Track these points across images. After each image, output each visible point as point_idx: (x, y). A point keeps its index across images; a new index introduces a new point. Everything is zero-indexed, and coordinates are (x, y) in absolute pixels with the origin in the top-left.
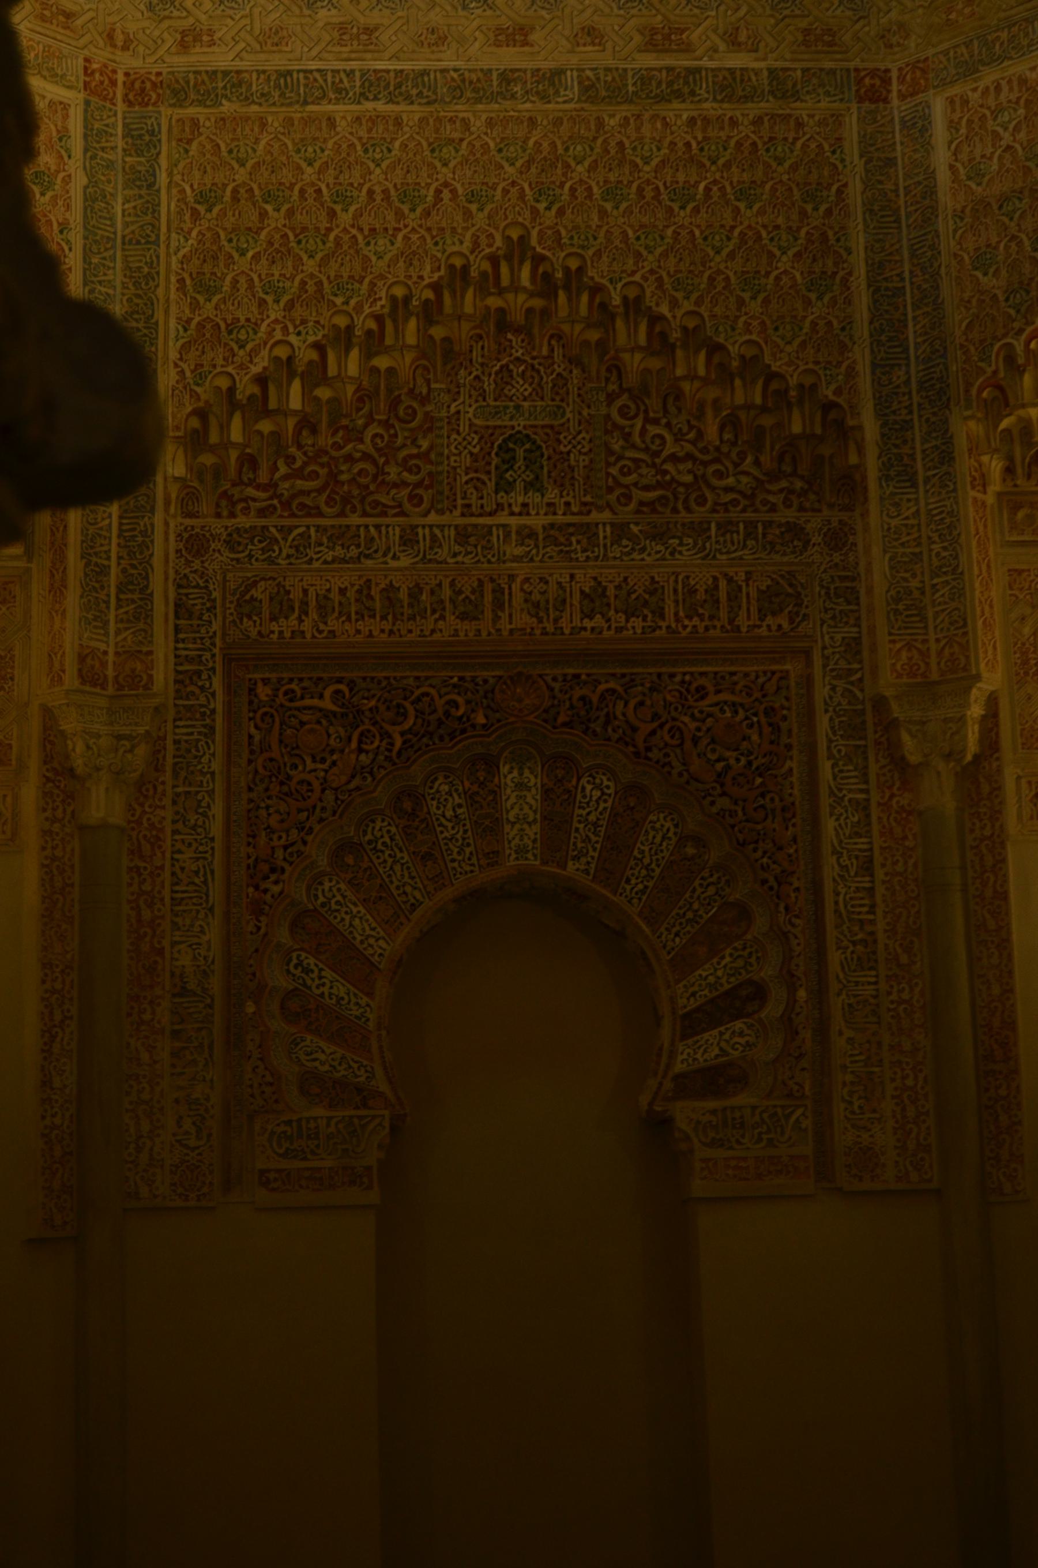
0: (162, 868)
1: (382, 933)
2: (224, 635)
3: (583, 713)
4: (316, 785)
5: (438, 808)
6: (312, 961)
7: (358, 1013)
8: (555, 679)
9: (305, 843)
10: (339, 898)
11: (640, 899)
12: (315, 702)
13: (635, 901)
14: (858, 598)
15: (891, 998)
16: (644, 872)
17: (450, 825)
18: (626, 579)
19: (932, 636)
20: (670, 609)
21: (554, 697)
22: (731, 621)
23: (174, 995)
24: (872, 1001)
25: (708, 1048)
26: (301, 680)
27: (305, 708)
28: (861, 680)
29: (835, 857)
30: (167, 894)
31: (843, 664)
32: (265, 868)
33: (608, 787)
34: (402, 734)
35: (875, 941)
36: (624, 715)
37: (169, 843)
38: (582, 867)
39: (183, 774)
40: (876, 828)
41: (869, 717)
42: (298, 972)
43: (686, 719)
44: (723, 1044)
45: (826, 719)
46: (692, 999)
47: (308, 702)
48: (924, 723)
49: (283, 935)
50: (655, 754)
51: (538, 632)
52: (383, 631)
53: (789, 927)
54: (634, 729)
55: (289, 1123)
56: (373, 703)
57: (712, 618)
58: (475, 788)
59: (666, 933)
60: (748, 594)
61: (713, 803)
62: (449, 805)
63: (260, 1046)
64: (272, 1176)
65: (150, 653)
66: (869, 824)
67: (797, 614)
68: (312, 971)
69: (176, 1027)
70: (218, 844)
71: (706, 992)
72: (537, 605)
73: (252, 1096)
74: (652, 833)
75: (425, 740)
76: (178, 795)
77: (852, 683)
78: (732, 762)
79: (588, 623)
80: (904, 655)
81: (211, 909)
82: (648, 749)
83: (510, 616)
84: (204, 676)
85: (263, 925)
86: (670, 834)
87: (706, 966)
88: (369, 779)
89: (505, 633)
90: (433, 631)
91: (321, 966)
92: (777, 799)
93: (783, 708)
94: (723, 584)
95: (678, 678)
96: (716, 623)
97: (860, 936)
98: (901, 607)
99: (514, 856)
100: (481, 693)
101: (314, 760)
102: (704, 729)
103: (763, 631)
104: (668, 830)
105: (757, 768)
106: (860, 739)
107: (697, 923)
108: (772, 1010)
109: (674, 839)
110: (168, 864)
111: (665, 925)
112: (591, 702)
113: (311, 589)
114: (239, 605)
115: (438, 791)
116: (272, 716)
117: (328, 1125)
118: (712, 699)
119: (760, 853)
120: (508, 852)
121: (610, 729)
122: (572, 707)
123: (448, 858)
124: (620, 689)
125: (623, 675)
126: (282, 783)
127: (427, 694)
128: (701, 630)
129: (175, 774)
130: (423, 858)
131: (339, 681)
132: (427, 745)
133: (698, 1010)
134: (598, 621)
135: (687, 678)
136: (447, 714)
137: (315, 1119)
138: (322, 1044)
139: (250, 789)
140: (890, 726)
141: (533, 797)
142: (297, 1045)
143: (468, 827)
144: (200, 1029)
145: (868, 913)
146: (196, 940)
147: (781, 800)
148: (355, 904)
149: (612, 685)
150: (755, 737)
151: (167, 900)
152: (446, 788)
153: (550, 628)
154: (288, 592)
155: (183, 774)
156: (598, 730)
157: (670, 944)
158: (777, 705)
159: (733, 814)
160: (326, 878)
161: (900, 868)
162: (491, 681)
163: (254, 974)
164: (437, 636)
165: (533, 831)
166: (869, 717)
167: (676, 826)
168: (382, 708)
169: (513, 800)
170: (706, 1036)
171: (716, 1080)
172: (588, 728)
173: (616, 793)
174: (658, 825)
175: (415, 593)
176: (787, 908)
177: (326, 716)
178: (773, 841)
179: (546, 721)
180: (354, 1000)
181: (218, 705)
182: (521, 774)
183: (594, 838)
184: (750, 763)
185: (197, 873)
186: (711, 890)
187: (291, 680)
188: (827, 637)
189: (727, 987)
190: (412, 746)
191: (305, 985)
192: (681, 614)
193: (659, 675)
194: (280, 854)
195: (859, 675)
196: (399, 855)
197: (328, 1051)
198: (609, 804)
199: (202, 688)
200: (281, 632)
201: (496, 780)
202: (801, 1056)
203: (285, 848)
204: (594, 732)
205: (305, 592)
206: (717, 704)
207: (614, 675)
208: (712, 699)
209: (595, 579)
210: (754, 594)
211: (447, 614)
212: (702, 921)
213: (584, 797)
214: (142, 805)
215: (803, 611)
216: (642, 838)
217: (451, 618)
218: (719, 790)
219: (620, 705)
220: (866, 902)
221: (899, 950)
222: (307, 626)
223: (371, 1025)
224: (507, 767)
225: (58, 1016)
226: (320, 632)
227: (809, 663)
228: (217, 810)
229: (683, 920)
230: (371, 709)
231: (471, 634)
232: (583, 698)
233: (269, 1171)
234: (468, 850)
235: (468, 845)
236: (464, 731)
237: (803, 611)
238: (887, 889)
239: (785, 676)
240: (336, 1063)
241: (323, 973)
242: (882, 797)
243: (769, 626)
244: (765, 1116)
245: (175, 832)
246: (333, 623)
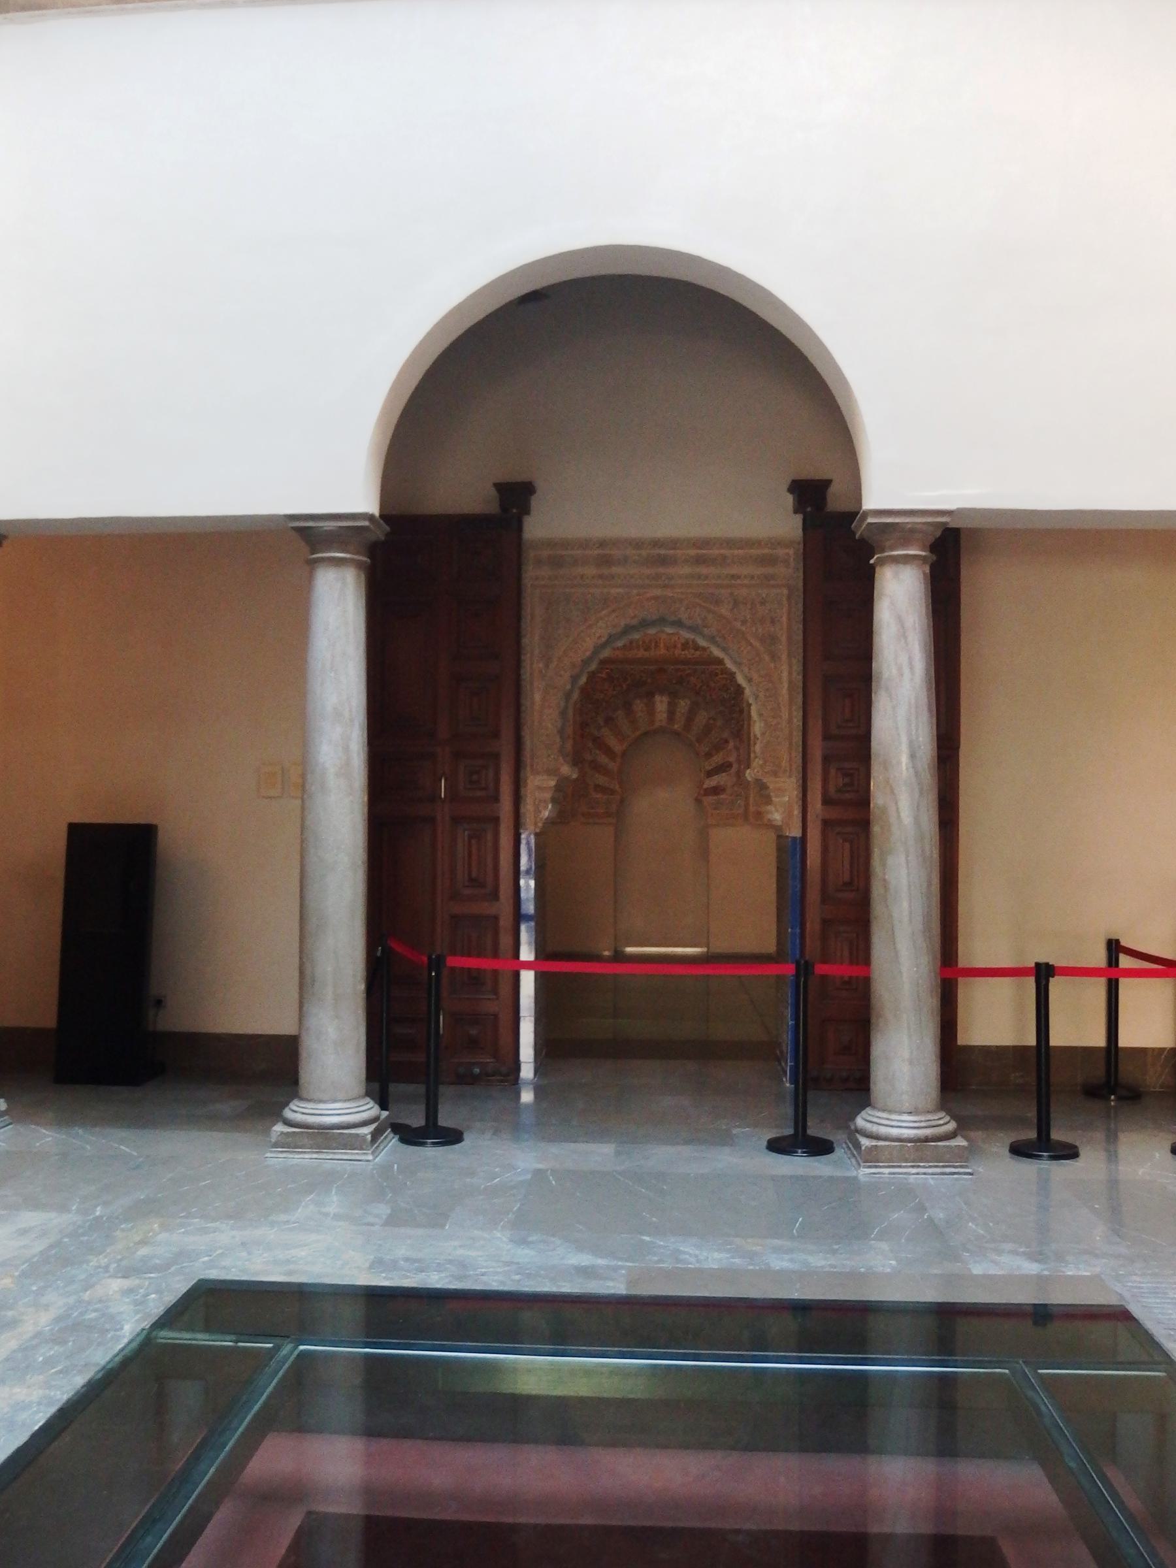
49: (590, 744)
165: (665, 715)
171: (716, 790)
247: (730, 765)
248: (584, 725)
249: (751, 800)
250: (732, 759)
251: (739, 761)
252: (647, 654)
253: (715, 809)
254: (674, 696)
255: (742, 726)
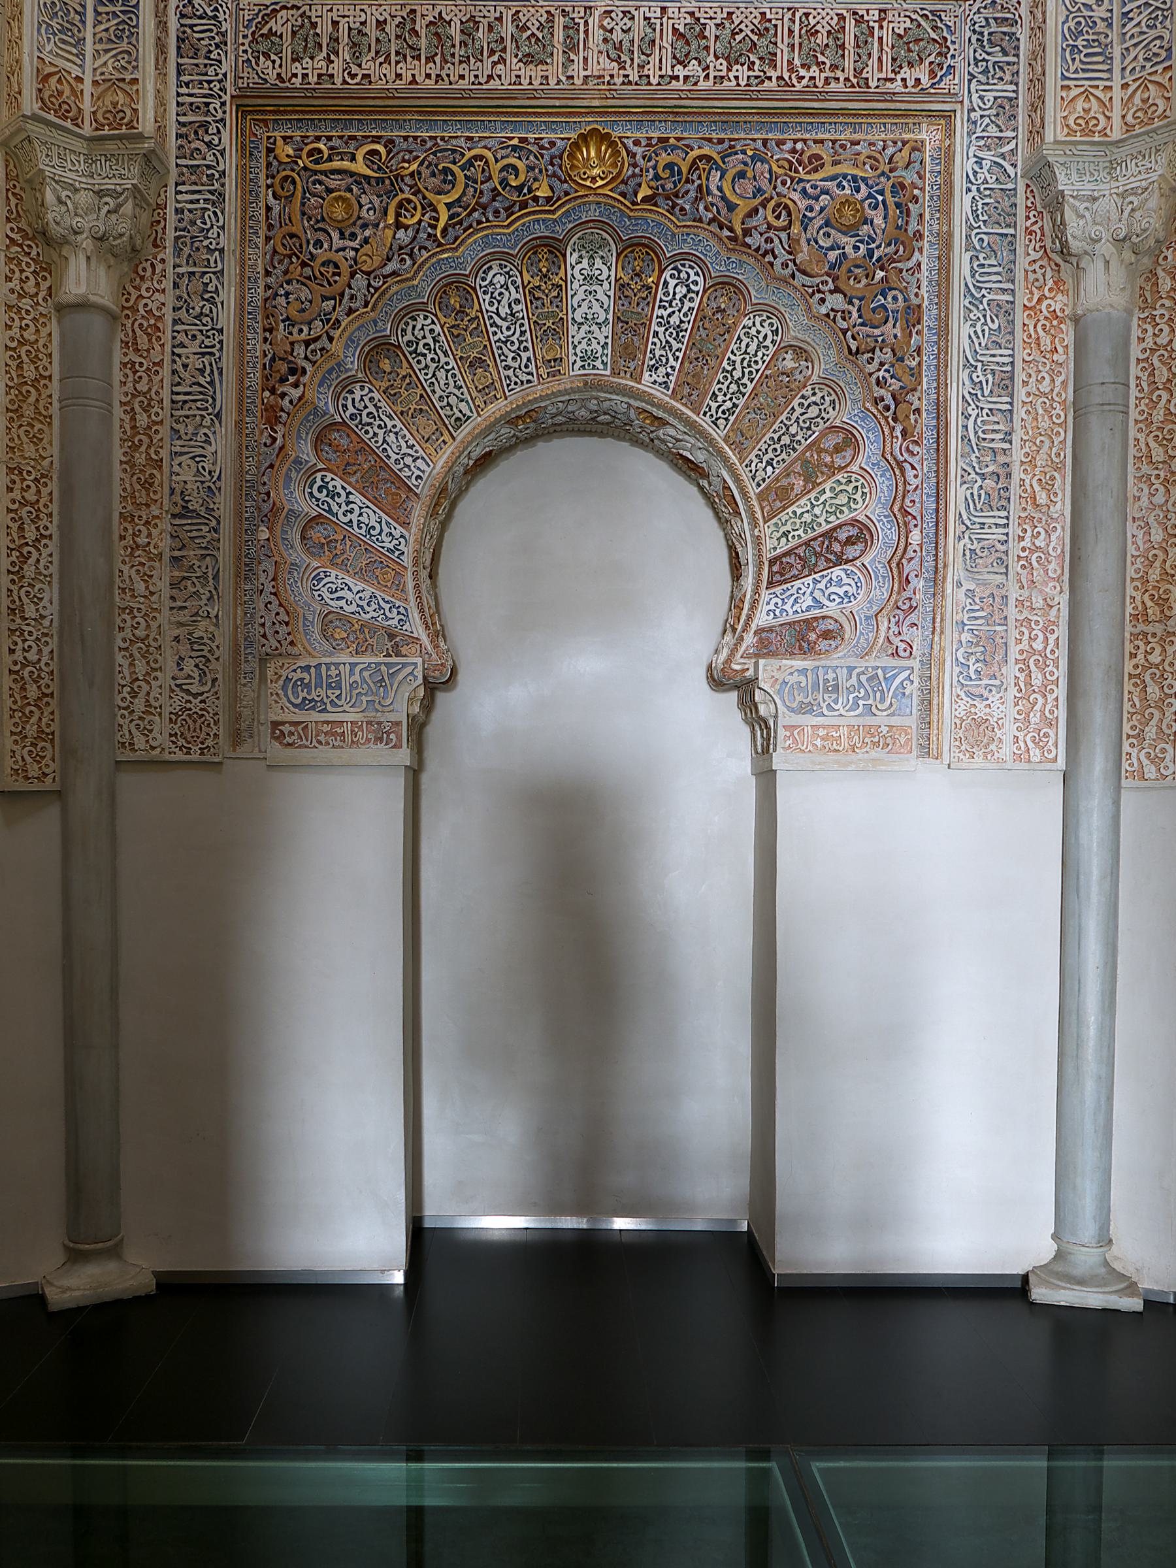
0: (160, 364)
1: (421, 452)
2: (237, 77)
3: (670, 186)
4: (345, 267)
5: (491, 304)
6: (339, 483)
7: (391, 546)
8: (637, 143)
9: (331, 339)
10: (372, 409)
11: (726, 419)
12: (346, 164)
13: (721, 422)
14: (1017, 48)
15: (1022, 544)
16: (734, 387)
17: (505, 325)
18: (730, 14)
19: (1117, 82)
20: (783, 58)
21: (635, 165)
22: (858, 73)
23: (174, 516)
24: (999, 546)
25: (800, 599)
26: (329, 138)
27: (333, 172)
28: (1013, 152)
29: (967, 371)
30: (166, 394)
31: (993, 131)
32: (283, 368)
33: (696, 283)
34: (449, 206)
35: (1009, 476)
36: (720, 189)
37: (169, 334)
38: (660, 380)
39: (187, 251)
40: (1019, 335)
41: (1020, 200)
42: (322, 496)
43: (796, 196)
44: (817, 594)
45: (967, 199)
46: (784, 540)
47: (336, 164)
48: (1095, 199)
49: (306, 451)
50: (755, 240)
51: (618, 80)
52: (428, 76)
53: (906, 455)
54: (732, 207)
55: (307, 669)
56: (414, 167)
57: (834, 67)
58: (536, 281)
59: (756, 461)
60: (880, 39)
61: (823, 300)
62: (505, 302)
63: (273, 580)
64: (286, 728)
65: (135, 81)
66: (1012, 333)
67: (940, 65)
68: (339, 495)
69: (177, 553)
70: (229, 338)
71: (801, 532)
72: (619, 47)
73: (264, 636)
74: (746, 340)
75: (476, 215)
76: (180, 276)
77: (1003, 156)
78: (849, 250)
79: (680, 71)
80: (1080, 104)
81: (218, 415)
82: (747, 232)
83: (585, 59)
84: (212, 129)
85: (279, 436)
86: (768, 342)
87: (802, 502)
88: (409, 262)
89: (578, 82)
90: (490, 77)
91: (349, 489)
92: (900, 297)
93: (914, 186)
94: (850, 24)
95: (789, 146)
96: (839, 74)
97: (991, 469)
98: (1080, 43)
99: (579, 363)
100: (547, 158)
101: (342, 236)
102: (817, 208)
103: (897, 86)
104: (765, 337)
105: (878, 260)
106: (1008, 226)
107: (794, 449)
108: (875, 556)
109: (772, 350)
110: (167, 358)
111: (756, 452)
112: (680, 172)
113: (343, 21)
114: (254, 40)
115: (491, 283)
116: (294, 182)
117: (351, 673)
118: (829, 171)
119: (875, 364)
120: (572, 358)
121: (701, 207)
122: (657, 177)
123: (501, 365)
124: (715, 155)
125: (721, 141)
126: (304, 264)
127: (480, 157)
128: (820, 83)
129: (178, 252)
130: (471, 365)
131: (376, 139)
132: (479, 222)
133: (787, 554)
134: (694, 68)
135: (799, 146)
136: (504, 182)
137: (337, 665)
138: (349, 581)
139: (268, 273)
140: (1055, 204)
141: (605, 292)
142: (320, 581)
143: (526, 327)
144: (204, 557)
145: (1003, 440)
146: (200, 451)
147: (905, 300)
148: (390, 417)
149: (706, 151)
150: (879, 221)
151: (167, 403)
152: (502, 280)
153: (634, 77)
154: (314, 25)
155: (187, 251)
156: (687, 207)
157: (761, 474)
158: (907, 182)
159: (846, 315)
160: (358, 386)
161: (1045, 387)
162: (559, 143)
163: (268, 494)
164: (492, 85)
166: (1020, 200)
167: (775, 333)
168: (426, 172)
169: (581, 295)
170: (797, 584)
171: (806, 636)
172: (674, 205)
173: (705, 291)
174: (753, 331)
175: (470, 27)
176: (904, 433)
177: (358, 183)
178: (893, 350)
179: (623, 195)
180: (386, 530)
181: (230, 163)
182: (592, 265)
183: (675, 345)
184: (870, 253)
185: (202, 371)
186: (813, 412)
187: (318, 139)
188: (975, 96)
189: (825, 527)
190: (461, 223)
191: (330, 511)
192: (797, 62)
193: (765, 142)
194: (300, 350)
195: (1012, 145)
196: (443, 359)
197: (355, 590)
198: (696, 304)
199: (209, 145)
200: (305, 76)
201: (562, 274)
202: (913, 609)
203: (307, 343)
204: (682, 209)
205: (335, 24)
206: (833, 178)
207: (710, 140)
208: (829, 171)
209: (692, 14)
210: (888, 39)
211: (508, 57)
212: (800, 448)
213: (666, 294)
214: (138, 288)
215: (949, 61)
216: (733, 346)
217: (512, 61)
218: (831, 286)
219: (716, 176)
220: (1001, 427)
221: (1037, 488)
222: (336, 68)
223: (407, 561)
224: (576, 255)
225: (31, 534)
226: (353, 76)
227: (950, 133)
228: (229, 295)
229: (778, 446)
230: (412, 175)
231: (536, 83)
232: (669, 166)
233: (283, 723)
234: (524, 355)
235: (526, 349)
236: (524, 205)
237: (949, 61)
238: (1028, 412)
239: (918, 147)
240: (364, 603)
241: (352, 498)
242: (1030, 300)
243: (904, 80)
244: (863, 678)
245: (175, 322)
246: (369, 65)
247: (862, 534)
248: (282, 371)
249: (950, 674)
250: (872, 509)
251: (903, 517)
252: (531, 75)
253: (806, 708)
254: (639, 252)
255: (916, 373)
